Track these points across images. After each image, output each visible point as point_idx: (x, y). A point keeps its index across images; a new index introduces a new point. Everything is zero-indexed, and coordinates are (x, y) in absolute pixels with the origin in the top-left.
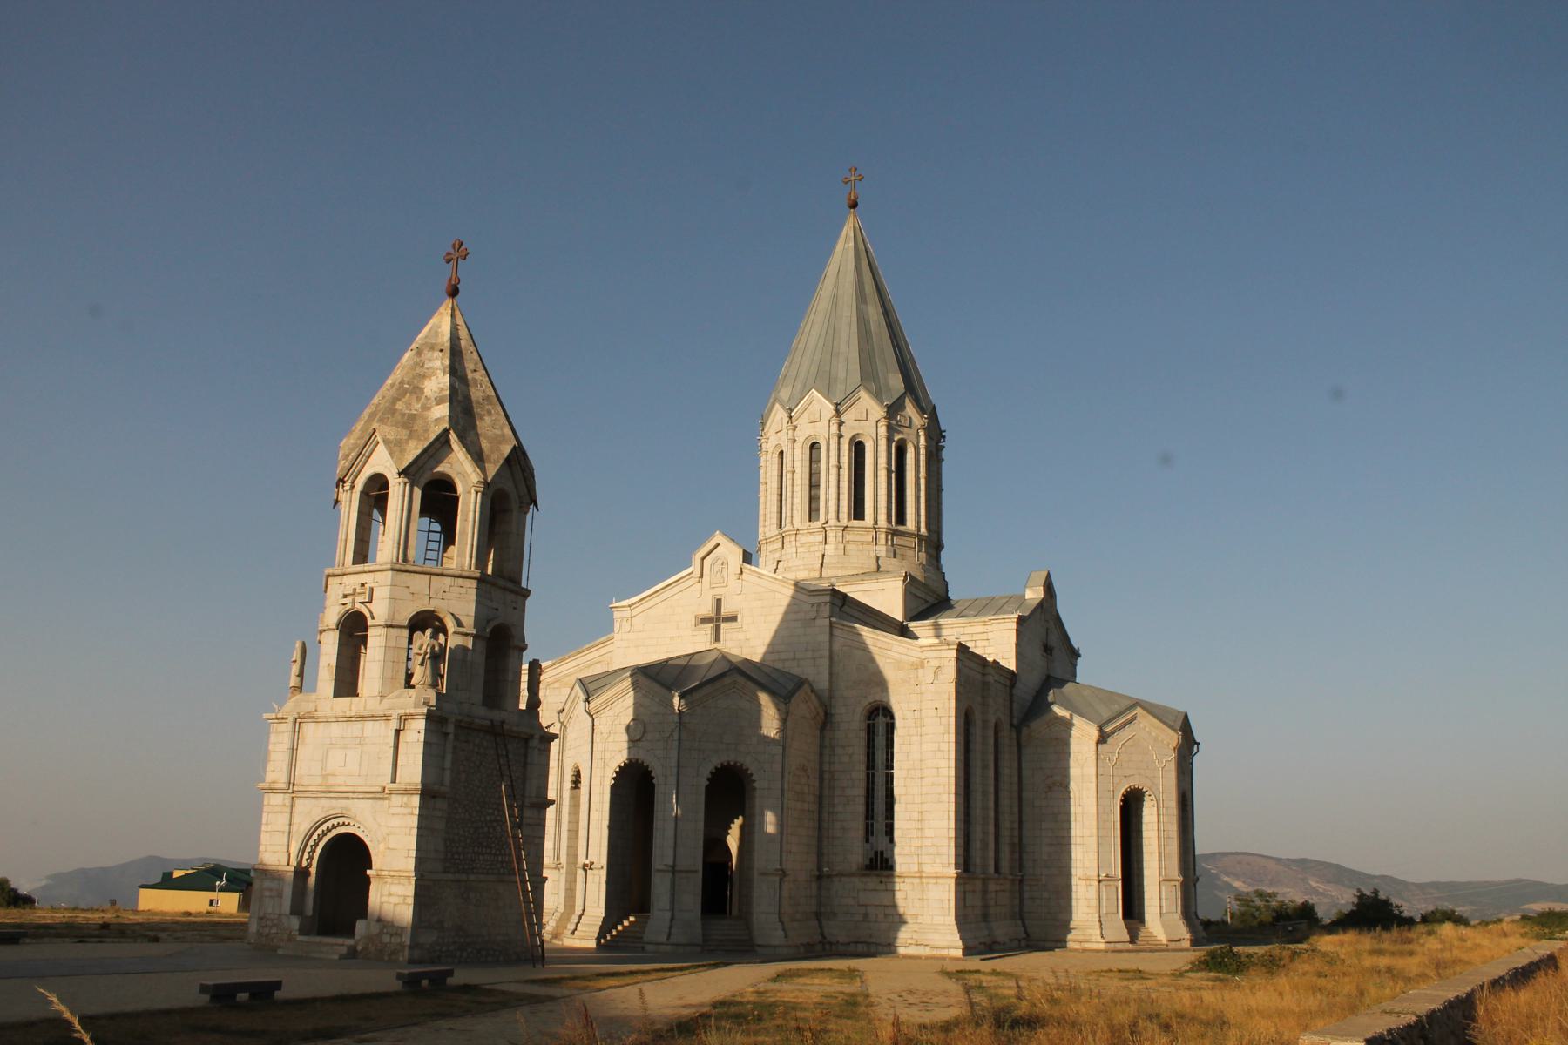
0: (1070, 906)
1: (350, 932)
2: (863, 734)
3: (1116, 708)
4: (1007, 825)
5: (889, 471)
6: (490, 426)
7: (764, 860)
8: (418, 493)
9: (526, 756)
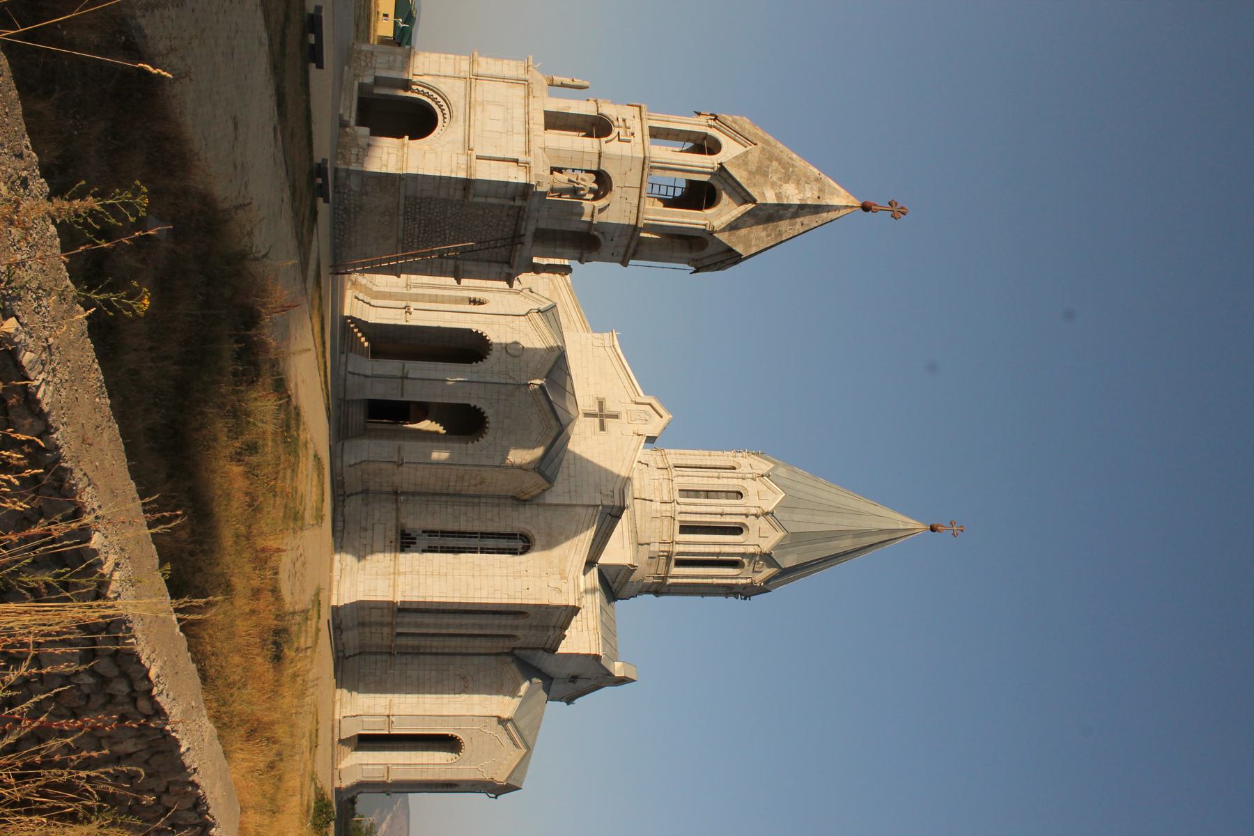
0: (369, 692)
1: (360, 123)
2: (509, 530)
3: (526, 733)
4: (435, 644)
5: (718, 554)
6: (758, 236)
7: (411, 449)
8: (705, 178)
9: (497, 262)
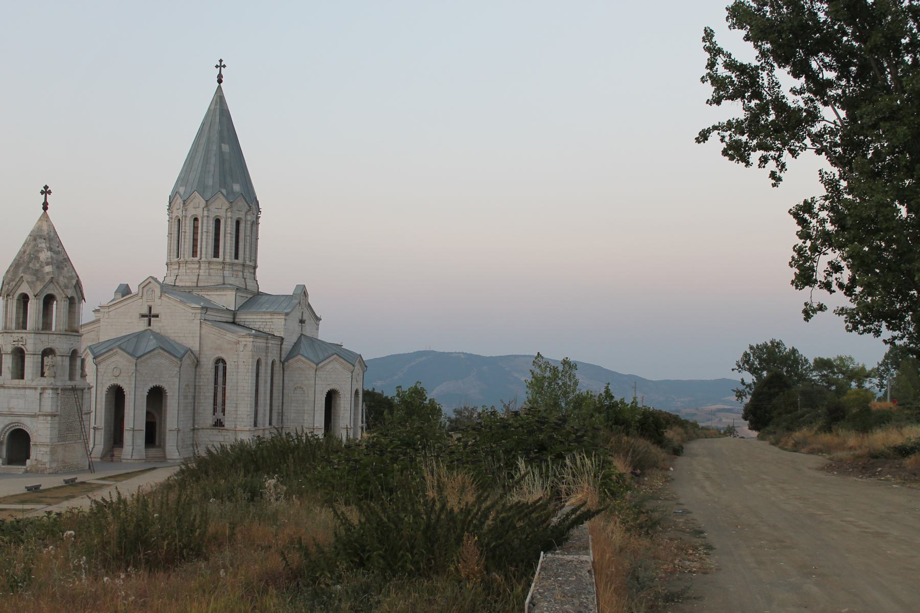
1: (24, 464)
2: (213, 370)
